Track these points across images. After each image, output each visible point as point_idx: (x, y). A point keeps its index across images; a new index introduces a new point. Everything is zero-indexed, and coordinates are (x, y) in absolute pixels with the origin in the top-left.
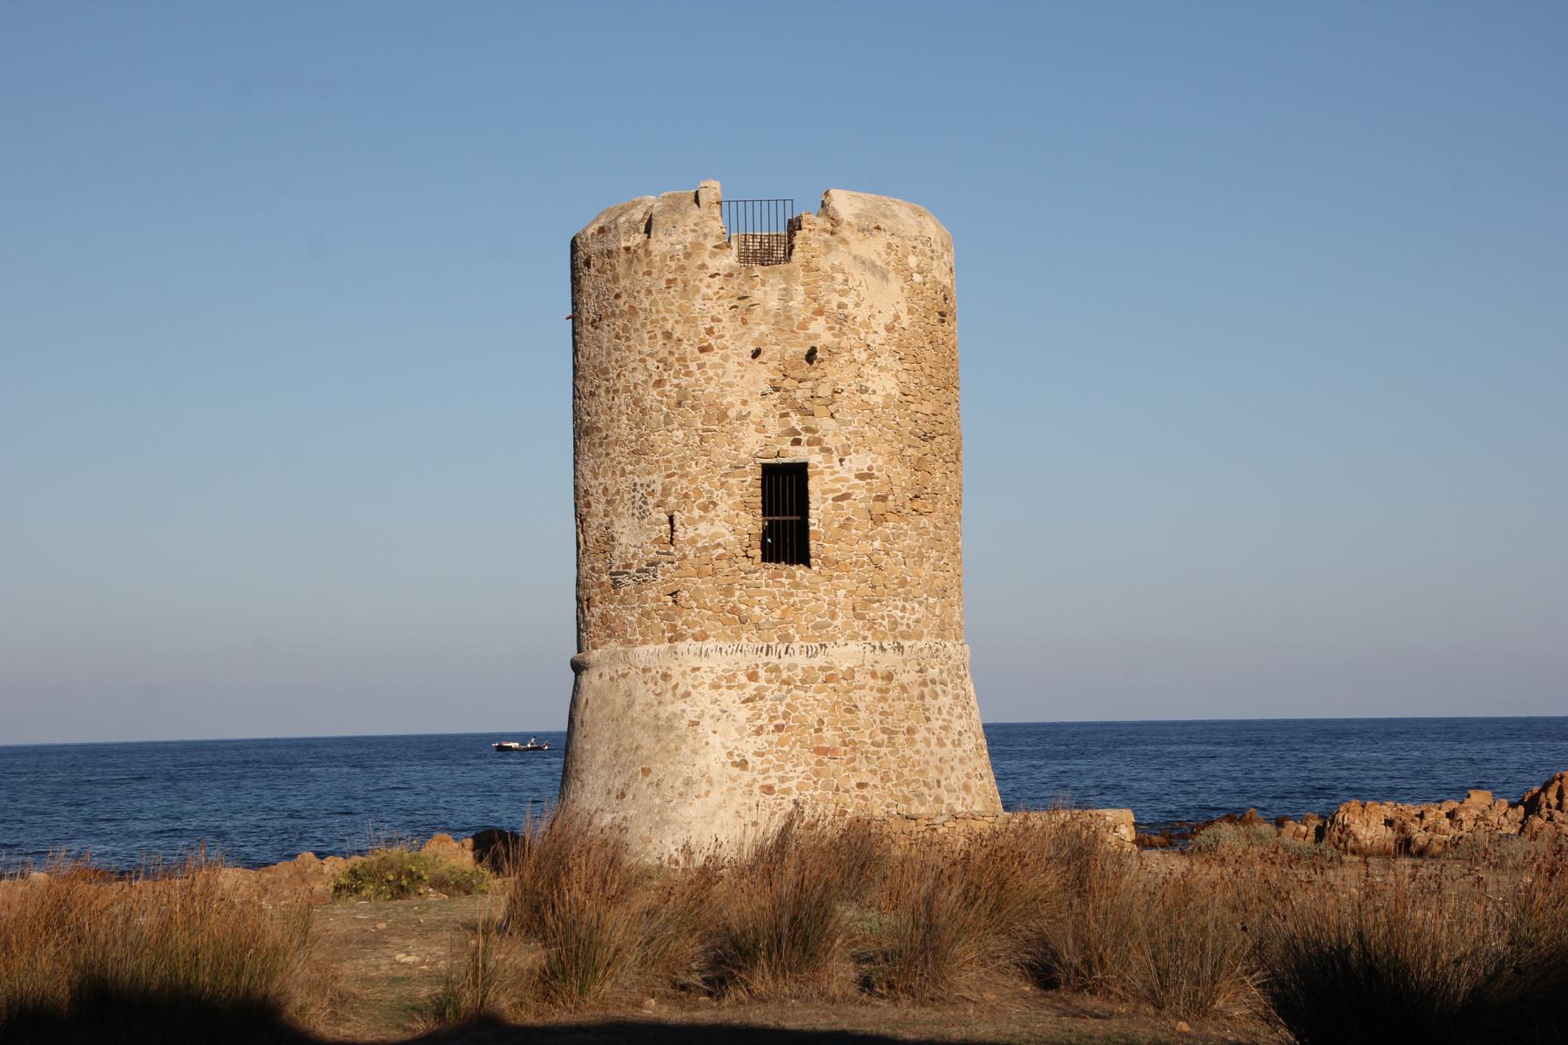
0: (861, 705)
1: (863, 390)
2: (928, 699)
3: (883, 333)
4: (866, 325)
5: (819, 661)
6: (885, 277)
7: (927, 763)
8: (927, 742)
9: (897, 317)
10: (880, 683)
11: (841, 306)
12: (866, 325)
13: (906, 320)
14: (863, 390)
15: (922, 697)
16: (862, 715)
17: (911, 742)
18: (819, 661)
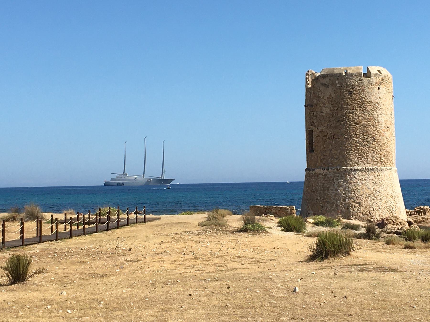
0: (320, 182)
1: (322, 112)
2: (335, 181)
3: (326, 99)
4: (323, 98)
5: (314, 172)
6: (328, 87)
7: (331, 194)
8: (332, 190)
9: (330, 95)
10: (323, 177)
11: (319, 94)
12: (323, 98)
13: (333, 95)
14: (322, 112)
15: (333, 180)
16: (320, 184)
17: (328, 190)
18: (314, 172)
